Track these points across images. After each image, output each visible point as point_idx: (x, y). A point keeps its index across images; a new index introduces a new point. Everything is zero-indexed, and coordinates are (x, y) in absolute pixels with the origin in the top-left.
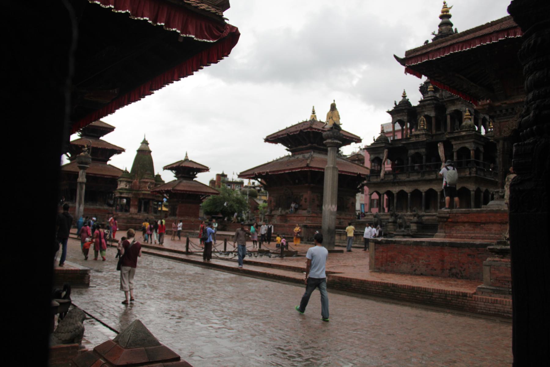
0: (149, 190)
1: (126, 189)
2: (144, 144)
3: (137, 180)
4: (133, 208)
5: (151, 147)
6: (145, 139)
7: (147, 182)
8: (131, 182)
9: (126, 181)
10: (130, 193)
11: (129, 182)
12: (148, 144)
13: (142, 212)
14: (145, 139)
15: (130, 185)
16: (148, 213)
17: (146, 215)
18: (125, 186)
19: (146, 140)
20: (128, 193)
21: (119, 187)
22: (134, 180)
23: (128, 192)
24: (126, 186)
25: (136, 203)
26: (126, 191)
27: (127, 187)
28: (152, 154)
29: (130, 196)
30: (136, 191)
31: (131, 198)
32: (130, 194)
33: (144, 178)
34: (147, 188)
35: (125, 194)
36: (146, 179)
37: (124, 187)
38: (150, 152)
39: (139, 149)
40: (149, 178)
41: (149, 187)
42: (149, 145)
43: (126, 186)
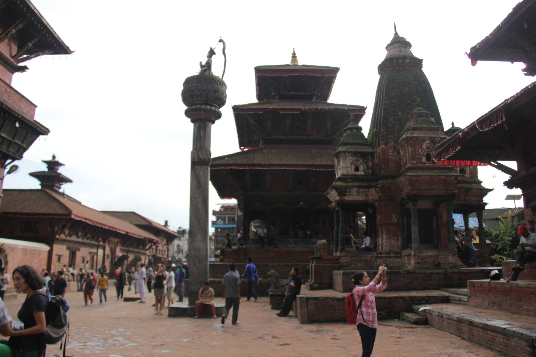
0: (428, 164)
1: (355, 178)
2: (395, 45)
3: (386, 144)
4: (385, 237)
5: (416, 52)
6: (396, 34)
7: (421, 141)
8: (372, 154)
9: (355, 154)
10: (369, 187)
11: (363, 155)
12: (408, 45)
13: (414, 245)
14: (396, 34)
15: (370, 164)
16: (436, 247)
17: (430, 253)
18: (353, 167)
19: (401, 35)
20: (364, 187)
21: (339, 174)
22: (379, 146)
23: (365, 184)
24: (357, 169)
25: (394, 219)
26: (355, 184)
27: (361, 173)
28: (426, 69)
29: (373, 195)
30: (386, 178)
31: (377, 204)
32: (373, 191)
33: (408, 130)
34: (424, 159)
35: (355, 189)
36: (415, 129)
37: (351, 171)
38: (418, 63)
39: (386, 58)
40: (425, 126)
41: (428, 158)
42: (412, 50)
43: (357, 169)
